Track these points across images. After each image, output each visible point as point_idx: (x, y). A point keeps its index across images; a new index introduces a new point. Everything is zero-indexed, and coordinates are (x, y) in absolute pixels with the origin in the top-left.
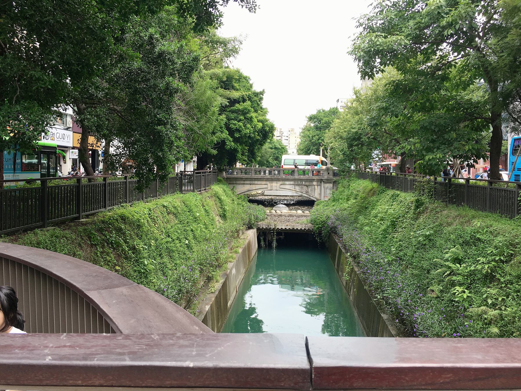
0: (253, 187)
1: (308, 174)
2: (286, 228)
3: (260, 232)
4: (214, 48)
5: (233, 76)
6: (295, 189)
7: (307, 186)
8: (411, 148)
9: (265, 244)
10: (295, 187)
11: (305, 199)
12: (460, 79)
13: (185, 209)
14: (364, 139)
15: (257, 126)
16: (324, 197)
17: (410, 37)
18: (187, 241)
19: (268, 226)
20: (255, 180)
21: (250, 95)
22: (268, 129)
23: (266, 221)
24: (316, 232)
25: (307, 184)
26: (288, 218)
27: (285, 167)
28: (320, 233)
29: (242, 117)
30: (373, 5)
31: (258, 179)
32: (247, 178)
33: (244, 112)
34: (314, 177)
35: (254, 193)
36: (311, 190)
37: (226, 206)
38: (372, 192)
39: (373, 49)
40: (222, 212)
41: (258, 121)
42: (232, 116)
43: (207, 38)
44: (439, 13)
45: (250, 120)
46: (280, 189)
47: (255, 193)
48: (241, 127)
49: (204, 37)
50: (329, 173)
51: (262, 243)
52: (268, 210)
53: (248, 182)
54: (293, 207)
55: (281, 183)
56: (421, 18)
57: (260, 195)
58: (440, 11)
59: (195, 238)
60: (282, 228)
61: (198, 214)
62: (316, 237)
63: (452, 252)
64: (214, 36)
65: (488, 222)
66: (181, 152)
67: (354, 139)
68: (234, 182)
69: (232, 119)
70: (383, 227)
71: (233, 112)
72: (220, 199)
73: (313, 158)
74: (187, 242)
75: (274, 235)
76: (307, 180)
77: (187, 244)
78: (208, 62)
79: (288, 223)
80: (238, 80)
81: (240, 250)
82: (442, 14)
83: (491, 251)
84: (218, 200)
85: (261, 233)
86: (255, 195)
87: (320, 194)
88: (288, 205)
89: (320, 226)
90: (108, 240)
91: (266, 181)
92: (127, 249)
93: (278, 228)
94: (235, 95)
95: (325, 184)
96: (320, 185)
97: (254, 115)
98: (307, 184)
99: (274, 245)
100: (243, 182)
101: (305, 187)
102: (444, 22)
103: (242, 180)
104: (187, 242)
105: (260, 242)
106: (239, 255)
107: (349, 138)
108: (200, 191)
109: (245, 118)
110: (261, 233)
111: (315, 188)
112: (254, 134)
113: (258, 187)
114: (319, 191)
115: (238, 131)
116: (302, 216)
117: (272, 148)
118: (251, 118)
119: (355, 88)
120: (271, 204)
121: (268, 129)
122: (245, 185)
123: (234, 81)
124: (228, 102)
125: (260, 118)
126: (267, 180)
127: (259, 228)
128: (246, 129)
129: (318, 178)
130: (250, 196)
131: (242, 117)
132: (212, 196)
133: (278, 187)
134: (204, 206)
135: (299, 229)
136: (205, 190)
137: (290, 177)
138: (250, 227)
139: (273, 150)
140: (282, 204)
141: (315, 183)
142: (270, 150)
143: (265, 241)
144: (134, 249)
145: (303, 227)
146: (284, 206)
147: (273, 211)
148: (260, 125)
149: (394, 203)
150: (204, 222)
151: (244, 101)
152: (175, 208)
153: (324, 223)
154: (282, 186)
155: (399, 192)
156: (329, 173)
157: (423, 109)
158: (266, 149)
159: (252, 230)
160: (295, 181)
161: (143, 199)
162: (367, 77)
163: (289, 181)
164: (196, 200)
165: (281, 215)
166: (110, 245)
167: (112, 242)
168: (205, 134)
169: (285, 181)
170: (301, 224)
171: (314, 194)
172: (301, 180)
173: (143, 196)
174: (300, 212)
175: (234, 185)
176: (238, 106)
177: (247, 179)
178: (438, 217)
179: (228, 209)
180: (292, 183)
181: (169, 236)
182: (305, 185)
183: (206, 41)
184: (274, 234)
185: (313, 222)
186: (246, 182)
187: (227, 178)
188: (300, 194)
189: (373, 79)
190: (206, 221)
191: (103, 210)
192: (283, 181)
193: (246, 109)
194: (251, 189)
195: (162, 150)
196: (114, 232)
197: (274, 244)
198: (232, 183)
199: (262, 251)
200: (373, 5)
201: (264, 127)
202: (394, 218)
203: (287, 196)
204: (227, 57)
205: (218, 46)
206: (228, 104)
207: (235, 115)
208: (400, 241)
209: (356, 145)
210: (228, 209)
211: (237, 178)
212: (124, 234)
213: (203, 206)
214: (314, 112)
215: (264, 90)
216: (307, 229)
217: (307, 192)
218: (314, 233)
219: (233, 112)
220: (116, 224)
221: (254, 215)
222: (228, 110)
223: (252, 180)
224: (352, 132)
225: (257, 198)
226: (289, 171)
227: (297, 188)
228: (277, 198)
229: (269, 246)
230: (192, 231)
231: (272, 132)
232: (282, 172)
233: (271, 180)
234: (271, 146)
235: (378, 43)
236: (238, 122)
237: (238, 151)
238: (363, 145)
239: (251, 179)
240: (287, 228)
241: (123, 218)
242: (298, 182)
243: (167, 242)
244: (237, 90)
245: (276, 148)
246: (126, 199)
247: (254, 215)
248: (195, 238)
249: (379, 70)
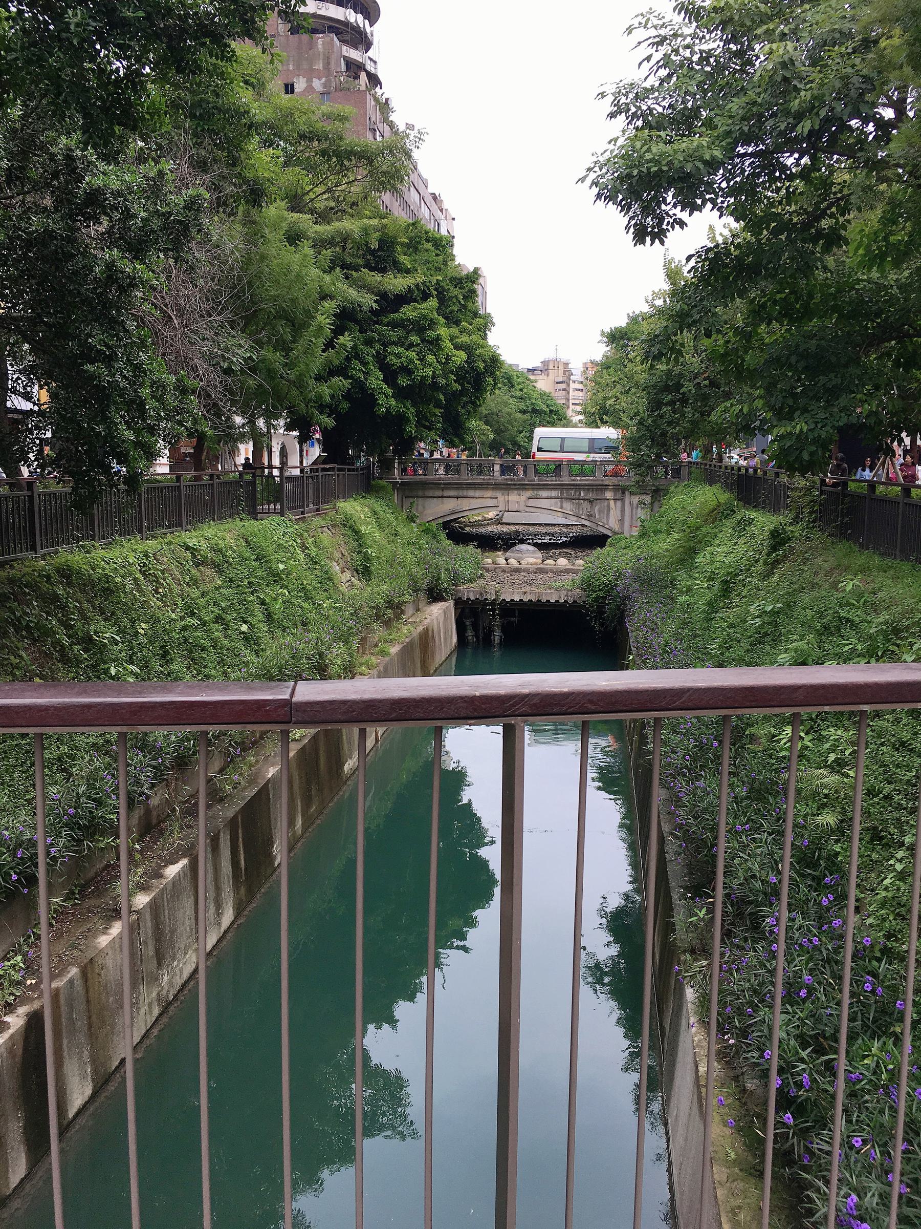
0: (465, 504)
1: (593, 473)
2: (521, 600)
3: (463, 609)
4: (343, 170)
5: (395, 238)
6: (562, 508)
7: (591, 501)
8: (741, 410)
9: (477, 636)
10: (562, 503)
11: (587, 532)
12: (885, 239)
13: (247, 555)
14: (688, 387)
15: (453, 358)
16: (631, 526)
17: (729, 140)
18: (244, 625)
19: (481, 594)
20: (468, 489)
21: (442, 284)
22: (481, 365)
23: (480, 582)
24: (591, 609)
25: (590, 495)
26: (532, 576)
27: (540, 456)
28: (600, 611)
29: (415, 339)
30: (653, 61)
31: (474, 484)
32: (449, 484)
33: (421, 326)
34: (607, 481)
35: (477, 518)
36: (600, 512)
37: (371, 547)
38: (718, 514)
39: (635, 172)
40: (359, 563)
41: (457, 347)
42: (393, 335)
43: (325, 145)
44: (785, 79)
45: (435, 343)
46: (528, 509)
47: (480, 518)
48: (411, 361)
49: (316, 143)
51: (470, 633)
52: (500, 558)
53: (452, 493)
54: (557, 551)
55: (529, 493)
56: (758, 90)
57: (492, 524)
58: (788, 75)
59: (269, 617)
60: (512, 600)
61: (281, 567)
62: (591, 619)
63: (796, 651)
64: (341, 139)
65: (879, 579)
66: (187, 422)
67: (666, 389)
68: (420, 493)
69: (394, 343)
70: (709, 596)
71: (394, 325)
72: (356, 532)
73: (608, 433)
74: (244, 628)
75: (494, 615)
76: (590, 488)
77: (243, 633)
78: (333, 204)
79: (528, 588)
80: (413, 246)
81: (394, 650)
82: (795, 82)
83: (851, 646)
84: (349, 533)
85: (467, 611)
86: (479, 524)
87: (621, 520)
88: (541, 547)
89: (601, 594)
90: (19, 620)
91: (493, 489)
92: (66, 641)
93: (504, 600)
94: (397, 283)
95: (633, 497)
96: (622, 500)
97: (443, 331)
98: (590, 495)
99: (497, 640)
100: (439, 493)
101: (586, 505)
102: (797, 101)
103: (438, 489)
104: (244, 628)
105: (465, 631)
106: (387, 659)
107: (654, 386)
108: (303, 513)
109: (423, 341)
110: (467, 611)
111: (609, 506)
112: (447, 379)
113: (475, 503)
114: (619, 513)
115: (407, 371)
116: (567, 571)
117: (524, 412)
118: (438, 338)
119: (670, 263)
120: (507, 542)
121: (481, 365)
123: (399, 248)
124: (375, 302)
125: (465, 339)
126: (497, 487)
127: (460, 598)
128: (424, 366)
129: (617, 483)
130: (465, 526)
131: (415, 339)
132: (334, 526)
133: (522, 504)
134: (307, 548)
135: (553, 601)
136: (318, 510)
137: (551, 479)
138: (435, 595)
139: (526, 417)
140: (529, 544)
141: (609, 494)
142: (519, 415)
143: (475, 627)
144: (88, 642)
145: (563, 596)
146: (531, 548)
147: (501, 561)
148: (461, 357)
149: (740, 541)
150: (302, 584)
151: (426, 296)
152: (218, 551)
153: (609, 587)
154: (532, 502)
155: (753, 515)
157: (787, 313)
158: (509, 414)
159: (442, 605)
160: (562, 490)
161: (140, 532)
162: (648, 239)
163: (548, 489)
164: (285, 533)
165: (517, 570)
166: (24, 633)
167: (28, 626)
168: (300, 377)
170: (558, 589)
171: (608, 521)
172: (578, 487)
173: (141, 526)
174: (562, 562)
175: (411, 500)
176: (408, 312)
178: (803, 570)
179: (374, 554)
180: (554, 493)
181: (192, 614)
182: (585, 499)
183: (324, 153)
184: (494, 613)
185: (587, 585)
186: (446, 493)
187: (402, 484)
188: (572, 521)
189: (662, 243)
190: (305, 583)
191: (30, 554)
192: (533, 489)
193: (424, 317)
194: (458, 509)
195: (105, 419)
196: (35, 604)
197: (497, 636)
198: (415, 494)
199: (469, 651)
200: (653, 61)
201: (474, 362)
202: (729, 573)
203: (555, 525)
204: (378, 191)
205: (354, 162)
206: (375, 306)
207: (401, 332)
208: (731, 626)
209: (666, 404)
210: (374, 554)
211: (426, 483)
212: (64, 608)
213: (304, 547)
214: (622, 322)
215: (476, 270)
216: (571, 600)
217: (590, 516)
218: (587, 610)
219: (394, 325)
220: (45, 587)
221: (447, 570)
222: (386, 320)
223: (463, 489)
224: (658, 372)
225: (482, 530)
226: (548, 465)
227: (568, 506)
228: (531, 529)
229: (487, 642)
230: (263, 603)
231: (492, 373)
232: (531, 470)
233: (507, 487)
234: (522, 406)
235: (648, 156)
236: (407, 349)
237: (408, 420)
238: (684, 401)
239: (460, 486)
240: (526, 600)
241: (66, 574)
242: (569, 492)
243: (184, 628)
244: (408, 271)
245: (535, 411)
246: (94, 531)
247: (447, 570)
248: (269, 617)
249: (675, 220)
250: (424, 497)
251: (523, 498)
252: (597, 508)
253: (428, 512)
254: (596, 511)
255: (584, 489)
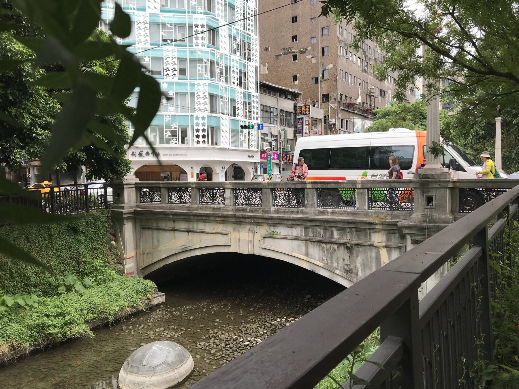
6: (307, 254)
7: (350, 248)
10: (307, 247)
20: (198, 221)
25: (348, 238)
31: (200, 215)
50: (430, 200)
53: (183, 226)
55: (263, 230)
68: (154, 225)
98: (348, 238)
100: (170, 225)
101: (342, 253)
103: (170, 220)
122: (178, 234)
126: (226, 219)
129: (389, 220)
141: (378, 238)
156: (430, 200)
160: (306, 227)
163: (287, 225)
169: (275, 225)
172: (327, 224)
177: (177, 217)
180: (296, 232)
182: (339, 244)
192: (268, 224)
223: (192, 221)
250: (158, 229)
251: (258, 237)
252: (359, 261)
253: (162, 247)
254: (359, 265)
255: (338, 228)
